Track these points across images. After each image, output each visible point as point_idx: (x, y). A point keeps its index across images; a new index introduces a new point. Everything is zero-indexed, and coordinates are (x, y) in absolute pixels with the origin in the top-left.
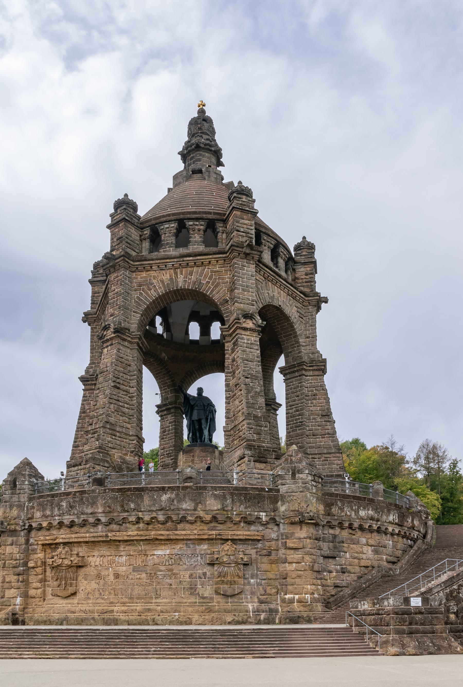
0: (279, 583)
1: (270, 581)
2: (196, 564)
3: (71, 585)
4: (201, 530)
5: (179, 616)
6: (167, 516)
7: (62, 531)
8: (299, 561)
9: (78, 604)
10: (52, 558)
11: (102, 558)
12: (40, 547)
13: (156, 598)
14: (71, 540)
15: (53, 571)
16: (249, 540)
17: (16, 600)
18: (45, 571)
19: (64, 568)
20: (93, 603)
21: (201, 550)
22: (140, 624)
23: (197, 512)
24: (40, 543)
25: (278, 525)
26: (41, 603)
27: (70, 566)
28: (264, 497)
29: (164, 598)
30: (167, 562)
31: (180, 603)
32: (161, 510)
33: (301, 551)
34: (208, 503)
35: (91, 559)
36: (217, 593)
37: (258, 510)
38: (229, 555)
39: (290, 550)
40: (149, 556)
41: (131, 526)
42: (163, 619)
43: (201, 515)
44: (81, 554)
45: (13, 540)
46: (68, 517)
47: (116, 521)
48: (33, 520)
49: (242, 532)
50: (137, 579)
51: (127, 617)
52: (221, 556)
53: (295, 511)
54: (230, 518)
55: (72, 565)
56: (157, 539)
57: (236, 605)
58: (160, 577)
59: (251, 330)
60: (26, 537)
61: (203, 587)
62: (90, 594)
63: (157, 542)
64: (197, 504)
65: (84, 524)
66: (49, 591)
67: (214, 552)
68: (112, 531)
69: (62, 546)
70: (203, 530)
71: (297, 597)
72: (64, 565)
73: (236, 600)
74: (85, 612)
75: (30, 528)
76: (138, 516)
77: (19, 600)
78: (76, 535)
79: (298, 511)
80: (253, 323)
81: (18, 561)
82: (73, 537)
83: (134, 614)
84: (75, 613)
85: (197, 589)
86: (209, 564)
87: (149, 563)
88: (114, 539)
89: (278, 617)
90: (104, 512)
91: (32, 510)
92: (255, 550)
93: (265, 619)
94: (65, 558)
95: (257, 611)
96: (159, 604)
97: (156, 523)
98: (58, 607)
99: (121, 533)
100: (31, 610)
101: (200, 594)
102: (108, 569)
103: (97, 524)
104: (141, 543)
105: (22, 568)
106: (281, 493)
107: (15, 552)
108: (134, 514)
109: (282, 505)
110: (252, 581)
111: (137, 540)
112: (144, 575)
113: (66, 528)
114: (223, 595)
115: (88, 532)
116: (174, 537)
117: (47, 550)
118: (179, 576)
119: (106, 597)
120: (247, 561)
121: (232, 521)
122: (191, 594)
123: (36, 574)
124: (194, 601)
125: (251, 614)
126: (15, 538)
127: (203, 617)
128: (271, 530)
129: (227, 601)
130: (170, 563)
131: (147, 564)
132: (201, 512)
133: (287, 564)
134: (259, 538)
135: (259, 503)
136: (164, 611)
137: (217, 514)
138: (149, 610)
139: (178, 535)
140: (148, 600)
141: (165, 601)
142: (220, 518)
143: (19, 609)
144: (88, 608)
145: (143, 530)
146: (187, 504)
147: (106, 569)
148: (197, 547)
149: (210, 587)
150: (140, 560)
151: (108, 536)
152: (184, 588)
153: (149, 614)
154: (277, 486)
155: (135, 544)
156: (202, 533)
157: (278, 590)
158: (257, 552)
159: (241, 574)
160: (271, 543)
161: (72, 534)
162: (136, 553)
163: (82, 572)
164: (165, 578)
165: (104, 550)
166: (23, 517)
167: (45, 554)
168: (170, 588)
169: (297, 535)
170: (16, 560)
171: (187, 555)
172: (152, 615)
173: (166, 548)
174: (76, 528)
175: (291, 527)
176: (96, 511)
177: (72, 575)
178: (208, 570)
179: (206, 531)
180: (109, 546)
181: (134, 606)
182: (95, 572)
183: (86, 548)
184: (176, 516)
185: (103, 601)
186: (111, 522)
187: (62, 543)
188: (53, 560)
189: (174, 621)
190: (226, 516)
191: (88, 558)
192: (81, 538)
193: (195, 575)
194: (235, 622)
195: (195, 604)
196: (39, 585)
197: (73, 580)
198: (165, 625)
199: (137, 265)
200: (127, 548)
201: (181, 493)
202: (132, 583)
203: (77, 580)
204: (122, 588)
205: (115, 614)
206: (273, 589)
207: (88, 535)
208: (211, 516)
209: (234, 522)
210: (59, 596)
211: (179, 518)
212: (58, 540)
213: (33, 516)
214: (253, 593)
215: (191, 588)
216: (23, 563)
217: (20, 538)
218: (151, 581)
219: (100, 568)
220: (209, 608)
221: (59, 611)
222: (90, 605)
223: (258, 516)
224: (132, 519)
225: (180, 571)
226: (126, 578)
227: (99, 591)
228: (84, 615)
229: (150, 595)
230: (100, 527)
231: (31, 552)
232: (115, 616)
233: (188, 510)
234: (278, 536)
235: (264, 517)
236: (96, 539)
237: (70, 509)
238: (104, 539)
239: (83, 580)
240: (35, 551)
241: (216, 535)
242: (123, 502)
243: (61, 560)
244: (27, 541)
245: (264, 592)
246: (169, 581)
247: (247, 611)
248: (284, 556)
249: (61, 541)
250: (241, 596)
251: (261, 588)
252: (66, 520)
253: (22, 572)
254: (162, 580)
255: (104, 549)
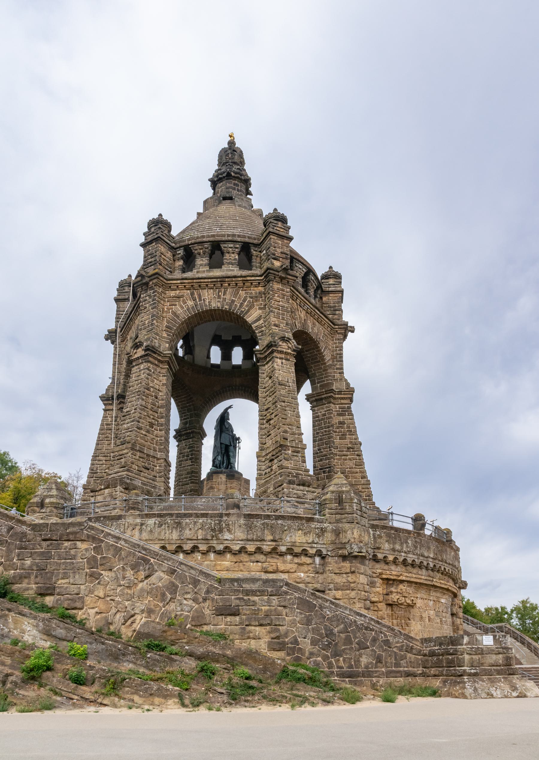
7: (399, 568)
48: (379, 551)
123: (377, 609)
249: (404, 578)
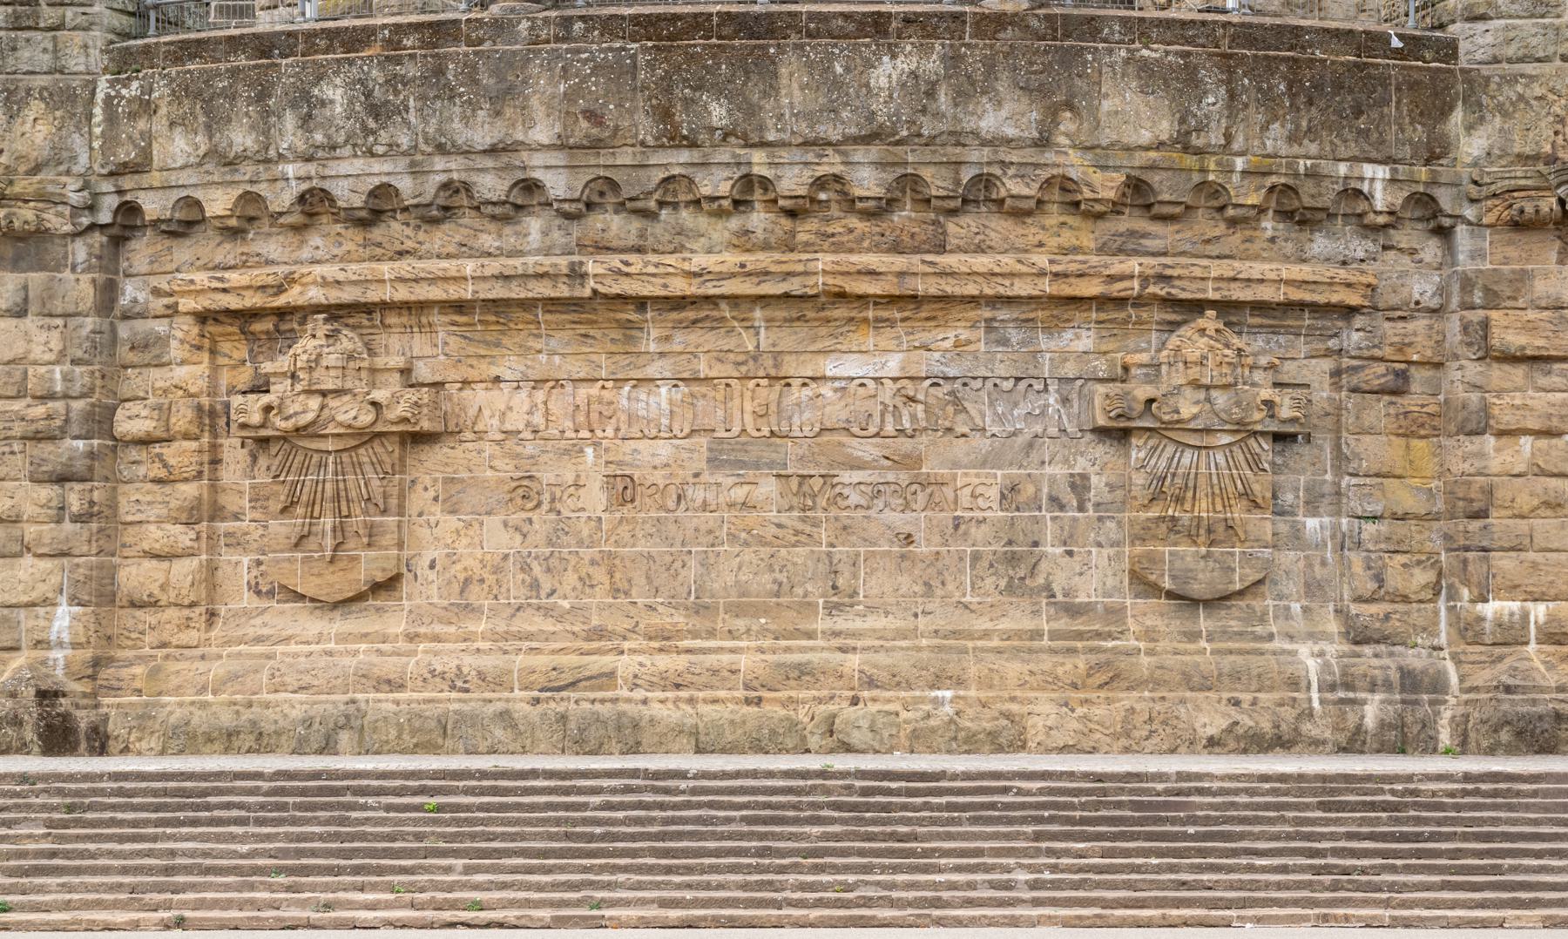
0: (1447, 537)
1: (1401, 529)
2: (1038, 429)
3: (372, 536)
4: (1065, 251)
5: (961, 706)
6: (900, 171)
7: (315, 239)
8: (1555, 422)
9: (412, 638)
10: (261, 388)
11: (540, 396)
12: (185, 328)
13: (832, 609)
14: (374, 295)
15: (263, 462)
16: (1302, 306)
17: (49, 619)
18: (215, 462)
19: (330, 445)
20: (495, 637)
21: (1064, 356)
22: (759, 748)
23: (1050, 157)
24: (187, 304)
25: (1443, 233)
26: (191, 636)
27: (369, 437)
28: (1384, 81)
29: (871, 609)
30: (889, 418)
31: (955, 634)
32: (866, 140)
33: (1562, 374)
34: (1106, 105)
35: (478, 397)
36: (1143, 584)
37: (1354, 150)
38: (1208, 388)
39: (1506, 367)
40: (796, 383)
41: (703, 222)
42: (881, 720)
43: (1073, 174)
44: (423, 372)
45: (25, 288)
46: (358, 165)
47: (626, 192)
48: (145, 180)
49: (1271, 267)
50: (731, 505)
51: (688, 709)
52: (1164, 388)
53: (1536, 158)
54: (1216, 191)
55: (379, 428)
56: (841, 296)
57: (1240, 652)
58: (855, 498)
60: (102, 269)
61: (1070, 553)
62: (475, 588)
63: (841, 312)
64: (1053, 113)
65: (445, 208)
66: (238, 567)
67: (1126, 369)
68: (602, 248)
69: (323, 329)
70: (1076, 250)
71: (1539, 611)
72: (331, 430)
73: (1235, 625)
74: (458, 682)
75: (128, 222)
76: (744, 170)
77: (63, 620)
78: (405, 267)
79: (1551, 159)
81: (59, 405)
82: (385, 278)
83: (722, 694)
84: (401, 687)
85: (1043, 566)
86: (1102, 433)
87: (796, 421)
88: (616, 290)
89: (1447, 715)
90: (561, 145)
91: (142, 124)
92: (1327, 365)
93: (1383, 725)
94: (339, 392)
95: (1344, 684)
96: (850, 642)
97: (835, 211)
98: (296, 655)
99: (653, 258)
100: (138, 670)
101: (1056, 588)
102: (576, 451)
103: (518, 208)
104: (758, 313)
105: (80, 444)
106: (1463, 63)
107: (37, 352)
108: (723, 155)
109: (1470, 128)
110: (1312, 523)
111: (734, 300)
112: (768, 488)
113: (338, 228)
114: (1170, 595)
115: (466, 250)
116: (931, 287)
117: (225, 347)
118: (948, 492)
119: (566, 604)
120: (1294, 420)
121: (1222, 209)
122: (1010, 589)
123: (162, 473)
124: (1028, 624)
125: (1315, 695)
126: (36, 278)
127: (1080, 711)
128: (1406, 259)
129: (1189, 626)
130: (907, 424)
131: (785, 429)
132: (1074, 156)
133: (1490, 441)
134: (1354, 299)
135: (1358, 112)
136: (883, 676)
137: (1153, 167)
138: (802, 673)
139: (952, 274)
140: (789, 619)
141: (880, 626)
142: (1165, 188)
143: (67, 666)
144: (469, 662)
145: (766, 247)
146: (1004, 113)
147: (566, 452)
148: (1044, 342)
149: (1106, 551)
150: (748, 407)
151: (584, 276)
152: (976, 557)
153: (804, 694)
154: (1442, 27)
155: (723, 318)
156: (1073, 267)
157: (1440, 574)
158: (1337, 373)
159: (1260, 488)
160: (1411, 326)
161: (373, 258)
162: (729, 370)
163: (432, 464)
164: (880, 503)
165: (557, 353)
166: (83, 159)
167: (215, 368)
168: (903, 557)
169: (1541, 287)
170: (50, 396)
171: (989, 384)
172: (820, 701)
173: (883, 344)
174: (395, 230)
175: (1510, 243)
176: (520, 136)
177: (375, 483)
178: (1096, 461)
179: (1094, 260)
180: (582, 329)
181: (720, 650)
182: (506, 466)
183: (452, 340)
184: (943, 171)
185: (549, 626)
186: (596, 199)
187: (317, 309)
188: (265, 399)
189: (933, 730)
190: (1196, 178)
191: (467, 393)
192: (433, 280)
193: (1031, 489)
194: (1238, 739)
195: (1036, 644)
196: (183, 536)
197: (384, 512)
198: (890, 751)
200: (680, 340)
201: (975, 52)
202: (703, 528)
203: (401, 511)
204: (650, 557)
205: (625, 693)
206: (1417, 571)
207: (470, 267)
208: (1120, 178)
209: (1230, 212)
210: (303, 597)
211: (957, 182)
212: (297, 289)
213: (146, 154)
214: (1313, 589)
215: (1012, 559)
216: (89, 416)
217: (67, 274)
218: (803, 520)
219: (530, 449)
220: (1108, 663)
221: (307, 679)
222: (481, 644)
223: (1353, 184)
224: (715, 183)
225: (956, 464)
226: (671, 504)
227: (525, 568)
228: (453, 703)
229: (799, 591)
230: (534, 226)
231: (132, 357)
232: (622, 706)
233: (1008, 141)
234: (1442, 291)
235: (1379, 186)
236: (516, 292)
237: (372, 124)
238: (563, 291)
239: (437, 508)
240: (156, 351)
241: (1145, 280)
242: (668, 90)
243: (314, 403)
244: (108, 293)
245: (1372, 585)
246: (898, 520)
247: (1294, 683)
248: (1475, 397)
249: (316, 295)
250: (1257, 604)
251: (1356, 559)
252: (345, 183)
253: (80, 466)
254: (860, 513)
255: (553, 343)
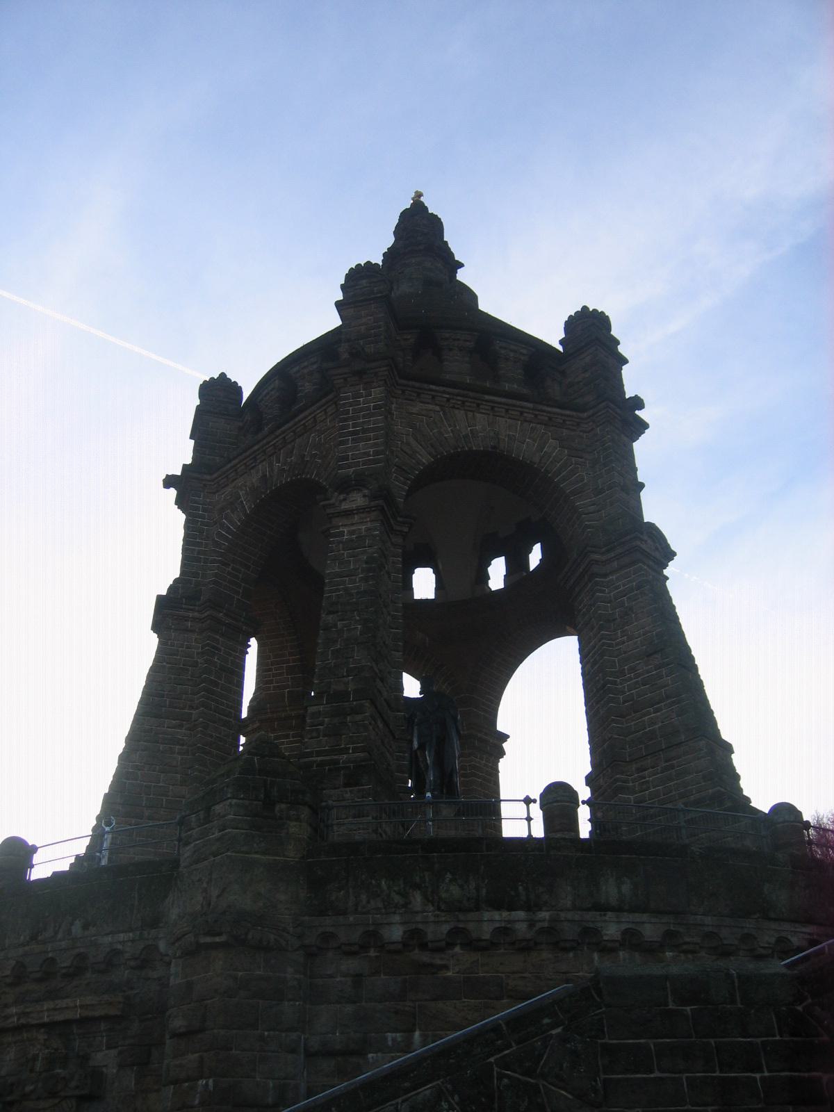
59: (360, 510)
80: (364, 496)
199: (216, 478)
